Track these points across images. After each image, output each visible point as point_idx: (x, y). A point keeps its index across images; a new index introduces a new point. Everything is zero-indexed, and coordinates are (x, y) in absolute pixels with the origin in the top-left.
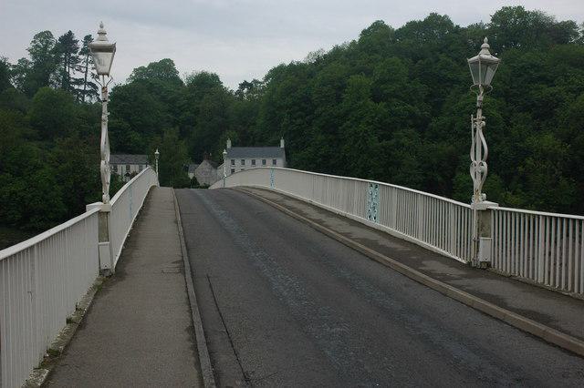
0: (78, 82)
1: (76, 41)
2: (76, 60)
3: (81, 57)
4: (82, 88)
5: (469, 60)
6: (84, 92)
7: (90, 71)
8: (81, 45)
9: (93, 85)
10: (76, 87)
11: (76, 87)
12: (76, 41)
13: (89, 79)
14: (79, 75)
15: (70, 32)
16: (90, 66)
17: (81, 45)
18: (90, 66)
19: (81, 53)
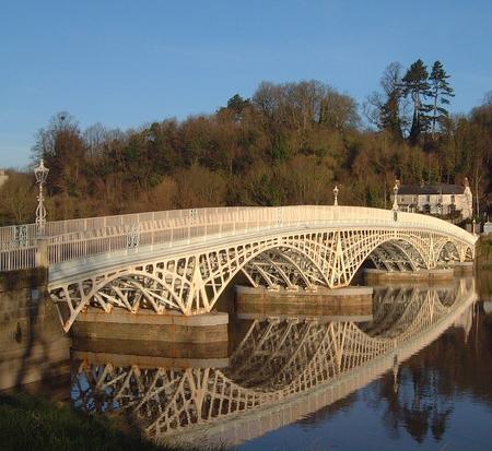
0: (430, 108)
2: (426, 86)
3: (430, 82)
4: (431, 114)
6: (434, 118)
7: (440, 96)
8: (429, 70)
9: (443, 110)
11: (425, 114)
12: (423, 68)
14: (429, 101)
15: (419, 61)
17: (429, 70)
18: (439, 91)
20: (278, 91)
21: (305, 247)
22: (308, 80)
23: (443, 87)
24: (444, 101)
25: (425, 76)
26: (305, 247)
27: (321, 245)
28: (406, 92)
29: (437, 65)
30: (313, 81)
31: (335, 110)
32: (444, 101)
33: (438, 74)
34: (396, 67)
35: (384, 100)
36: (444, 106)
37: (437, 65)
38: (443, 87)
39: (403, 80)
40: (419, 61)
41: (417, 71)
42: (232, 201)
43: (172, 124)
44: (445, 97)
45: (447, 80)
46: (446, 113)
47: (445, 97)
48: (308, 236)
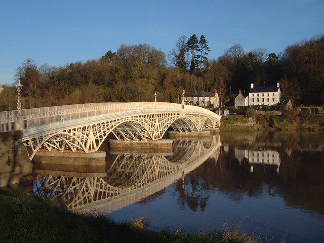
0: (199, 56)
2: (197, 47)
3: (199, 45)
4: (200, 59)
6: (201, 61)
7: (204, 51)
8: (199, 39)
9: (205, 58)
11: (197, 59)
14: (199, 53)
17: (199, 39)
20: (129, 49)
21: (141, 121)
22: (143, 44)
24: (206, 53)
25: (197, 41)
26: (141, 121)
27: (149, 120)
28: (188, 49)
29: (202, 37)
30: (145, 44)
31: (155, 58)
32: (206, 53)
33: (203, 41)
34: (183, 38)
35: (178, 53)
37: (202, 37)
40: (194, 35)
41: (193, 40)
42: (108, 99)
43: (79, 64)
44: (206, 51)
45: (207, 44)
46: (207, 59)
47: (206, 51)
48: (143, 116)
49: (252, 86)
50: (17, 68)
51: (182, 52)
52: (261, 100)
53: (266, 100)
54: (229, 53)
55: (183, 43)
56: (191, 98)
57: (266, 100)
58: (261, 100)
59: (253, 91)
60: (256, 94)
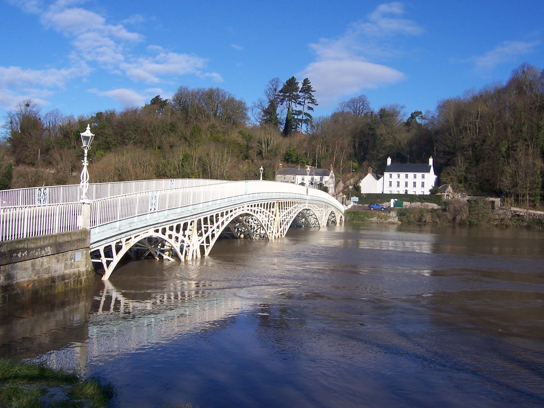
0: (300, 113)
1: (297, 83)
2: (298, 97)
3: (301, 94)
4: (300, 117)
5: (82, 134)
6: (301, 121)
7: (307, 105)
8: (300, 86)
9: (309, 115)
10: (296, 117)
11: (296, 117)
13: (306, 111)
14: (299, 108)
16: (306, 101)
17: (300, 86)
18: (306, 101)
19: (300, 92)
20: (194, 95)
22: (215, 87)
23: (310, 98)
24: (310, 108)
27: (268, 212)
28: (282, 101)
30: (218, 89)
32: (310, 108)
33: (307, 89)
34: (276, 81)
36: (309, 112)
38: (310, 98)
39: (280, 92)
42: (161, 175)
43: (112, 114)
44: (310, 105)
45: (313, 94)
46: (310, 117)
47: (310, 105)
49: (389, 161)
50: (6, 115)
51: (273, 106)
52: (402, 184)
53: (410, 185)
54: (347, 110)
55: (275, 90)
56: (292, 176)
57: (410, 185)
58: (402, 184)
59: (392, 169)
60: (395, 175)
